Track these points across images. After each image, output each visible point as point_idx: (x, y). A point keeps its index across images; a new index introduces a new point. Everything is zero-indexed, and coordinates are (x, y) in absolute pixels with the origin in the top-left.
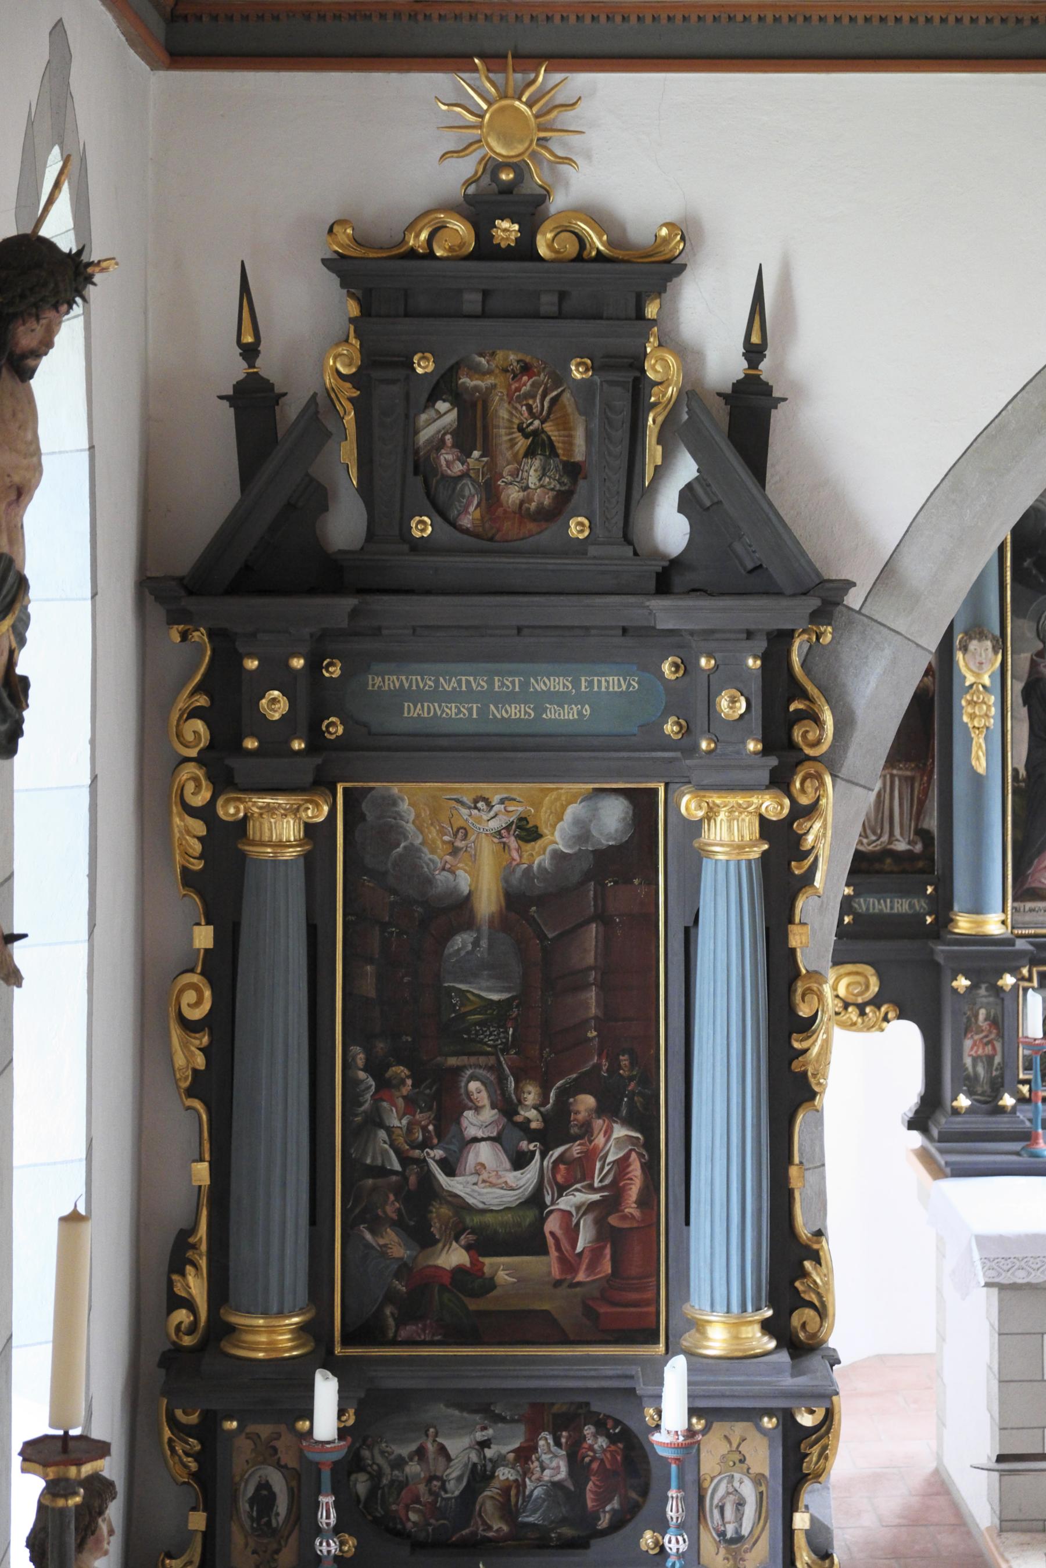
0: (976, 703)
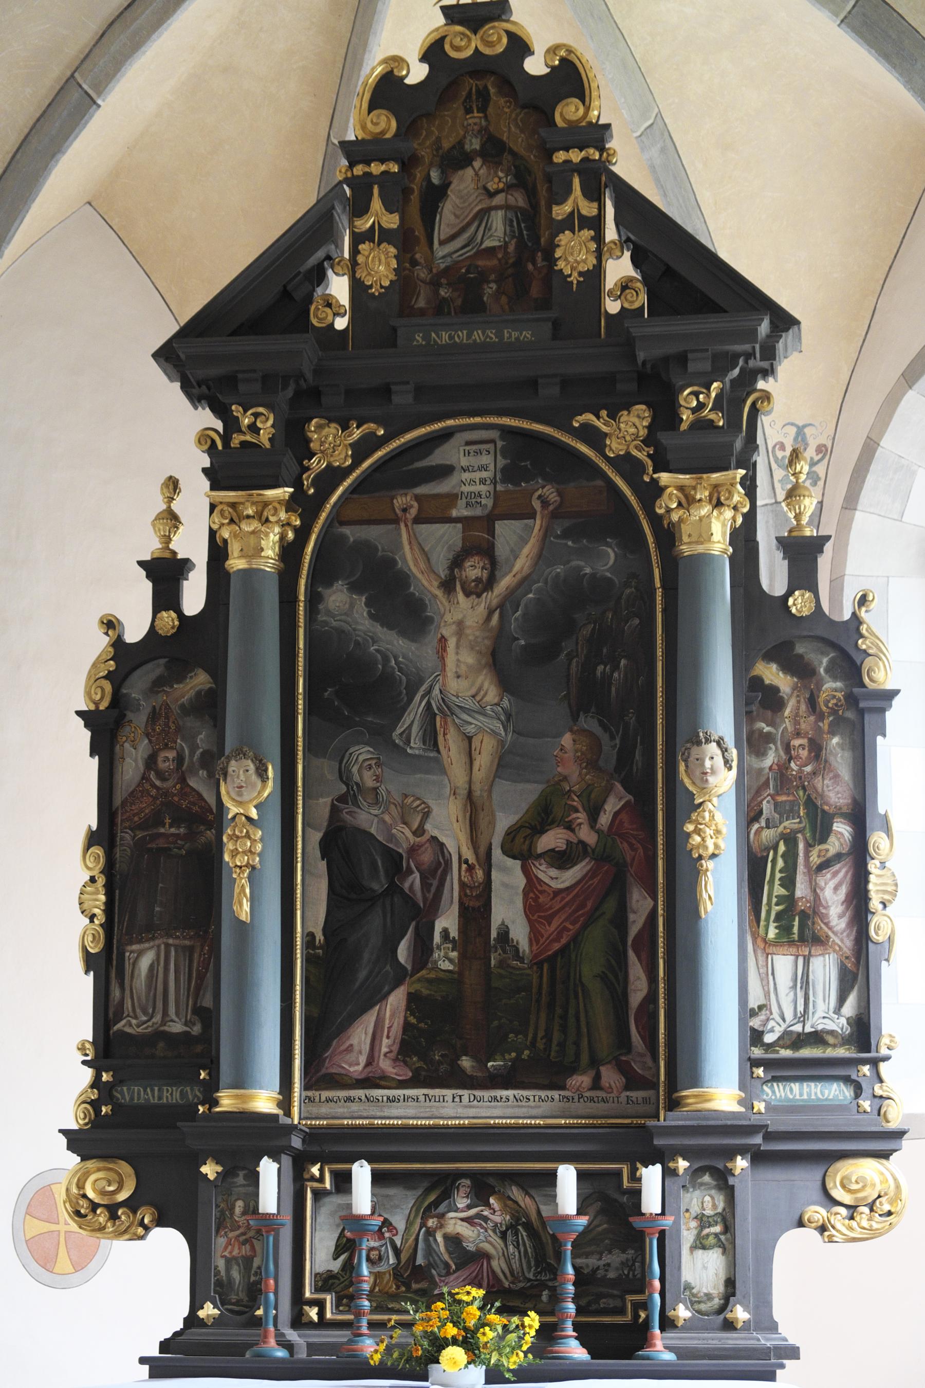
0: (238, 837)
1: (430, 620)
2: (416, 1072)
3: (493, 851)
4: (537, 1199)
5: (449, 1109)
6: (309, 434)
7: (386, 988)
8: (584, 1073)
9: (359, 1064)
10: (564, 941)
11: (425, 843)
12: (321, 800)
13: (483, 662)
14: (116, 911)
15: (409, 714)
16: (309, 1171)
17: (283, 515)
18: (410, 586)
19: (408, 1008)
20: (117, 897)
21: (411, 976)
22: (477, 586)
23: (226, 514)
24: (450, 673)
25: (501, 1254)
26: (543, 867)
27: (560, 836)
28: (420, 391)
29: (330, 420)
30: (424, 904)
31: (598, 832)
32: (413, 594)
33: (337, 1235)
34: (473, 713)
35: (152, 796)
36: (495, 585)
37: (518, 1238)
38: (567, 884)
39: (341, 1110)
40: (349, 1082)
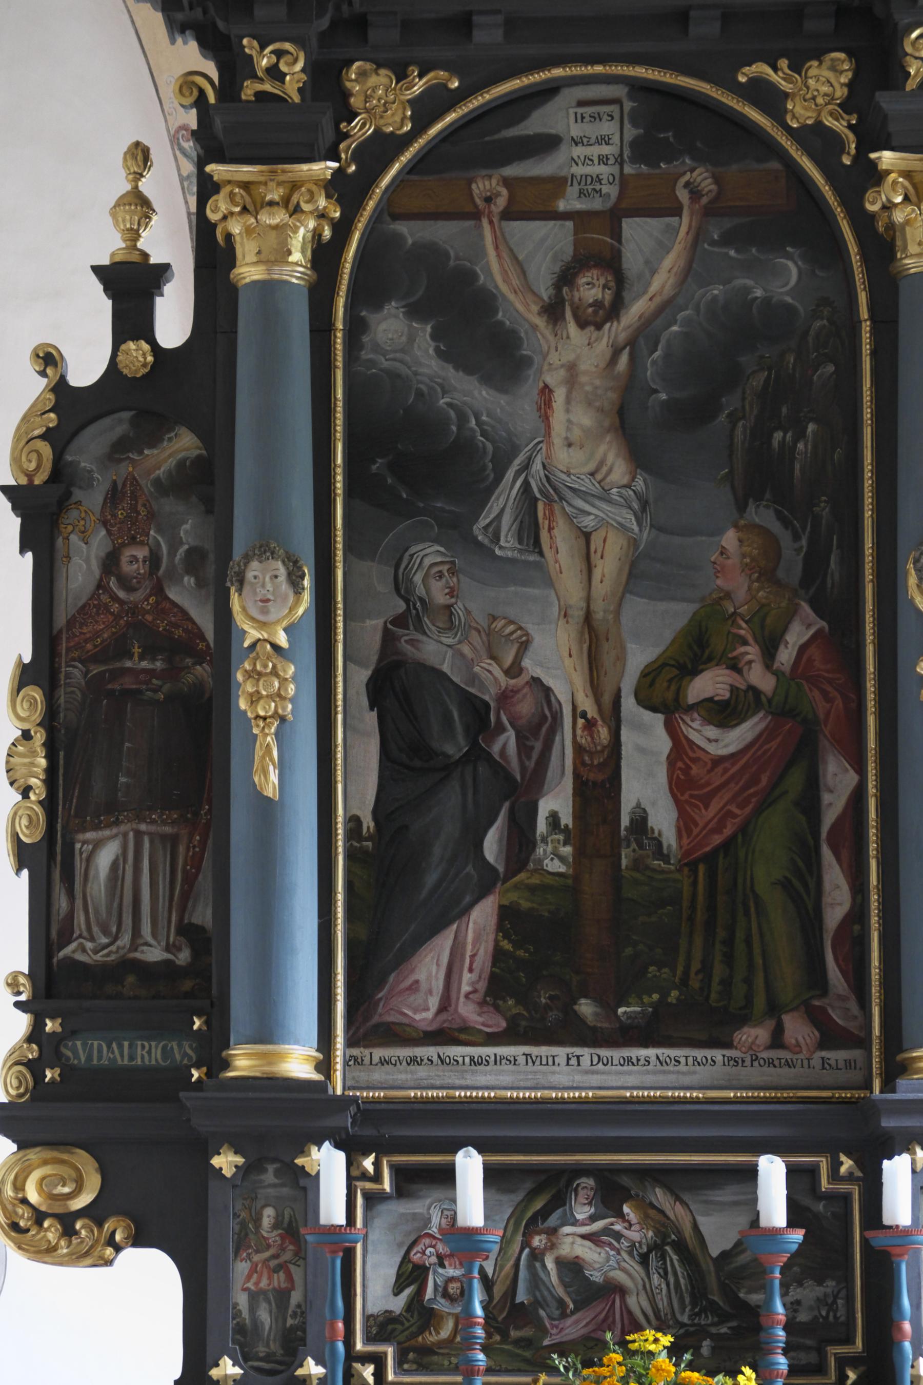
1: (527, 362)
2: (513, 1022)
3: (622, 700)
4: (692, 1208)
5: (562, 1075)
6: (348, 84)
7: (468, 899)
8: (758, 1023)
9: (428, 1009)
10: (728, 831)
11: (523, 687)
12: (369, 623)
13: (607, 423)
14: (61, 782)
15: (498, 499)
16: (360, 1165)
17: (322, 202)
18: (497, 312)
19: (500, 927)
20: (61, 762)
21: (504, 882)
22: (595, 313)
23: (238, 199)
24: (557, 441)
25: (640, 1287)
26: (696, 725)
27: (720, 679)
28: (512, 25)
29: (379, 65)
30: (523, 777)
31: (777, 674)
32: (501, 323)
33: (398, 1259)
34: (590, 499)
35: (112, 614)
36: (623, 312)
37: (665, 1263)
38: (732, 749)
39: (402, 1077)
40: (414, 1034)
